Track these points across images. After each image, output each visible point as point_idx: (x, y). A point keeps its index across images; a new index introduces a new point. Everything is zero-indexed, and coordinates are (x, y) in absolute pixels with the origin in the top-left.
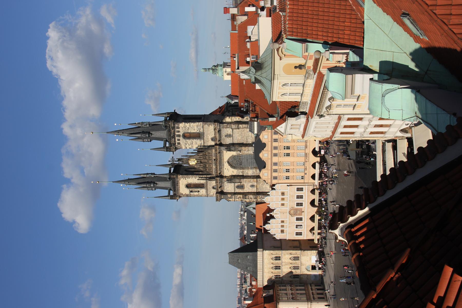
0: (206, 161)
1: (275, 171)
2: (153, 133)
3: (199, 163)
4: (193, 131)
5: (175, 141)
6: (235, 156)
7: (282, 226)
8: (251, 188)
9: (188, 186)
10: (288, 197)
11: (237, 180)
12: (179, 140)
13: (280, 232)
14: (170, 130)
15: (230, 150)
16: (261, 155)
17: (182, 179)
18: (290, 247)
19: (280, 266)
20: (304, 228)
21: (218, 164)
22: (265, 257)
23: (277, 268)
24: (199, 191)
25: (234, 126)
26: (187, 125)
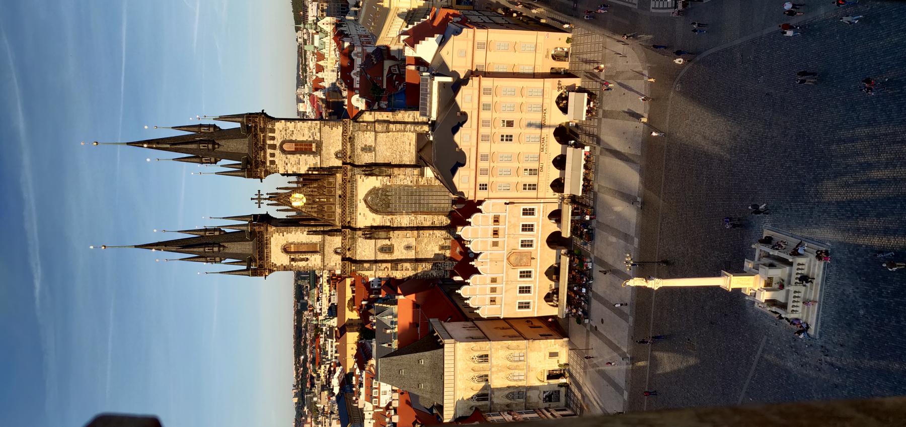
1: (485, 172)
2: (222, 142)
4: (300, 138)
5: (265, 157)
6: (379, 189)
7: (493, 290)
8: (405, 252)
11: (383, 234)
12: (273, 155)
13: (488, 301)
14: (256, 135)
15: (371, 175)
16: (457, 138)
17: (276, 235)
20: (535, 292)
22: (458, 357)
24: (307, 259)
25: (379, 127)
26: (291, 125)
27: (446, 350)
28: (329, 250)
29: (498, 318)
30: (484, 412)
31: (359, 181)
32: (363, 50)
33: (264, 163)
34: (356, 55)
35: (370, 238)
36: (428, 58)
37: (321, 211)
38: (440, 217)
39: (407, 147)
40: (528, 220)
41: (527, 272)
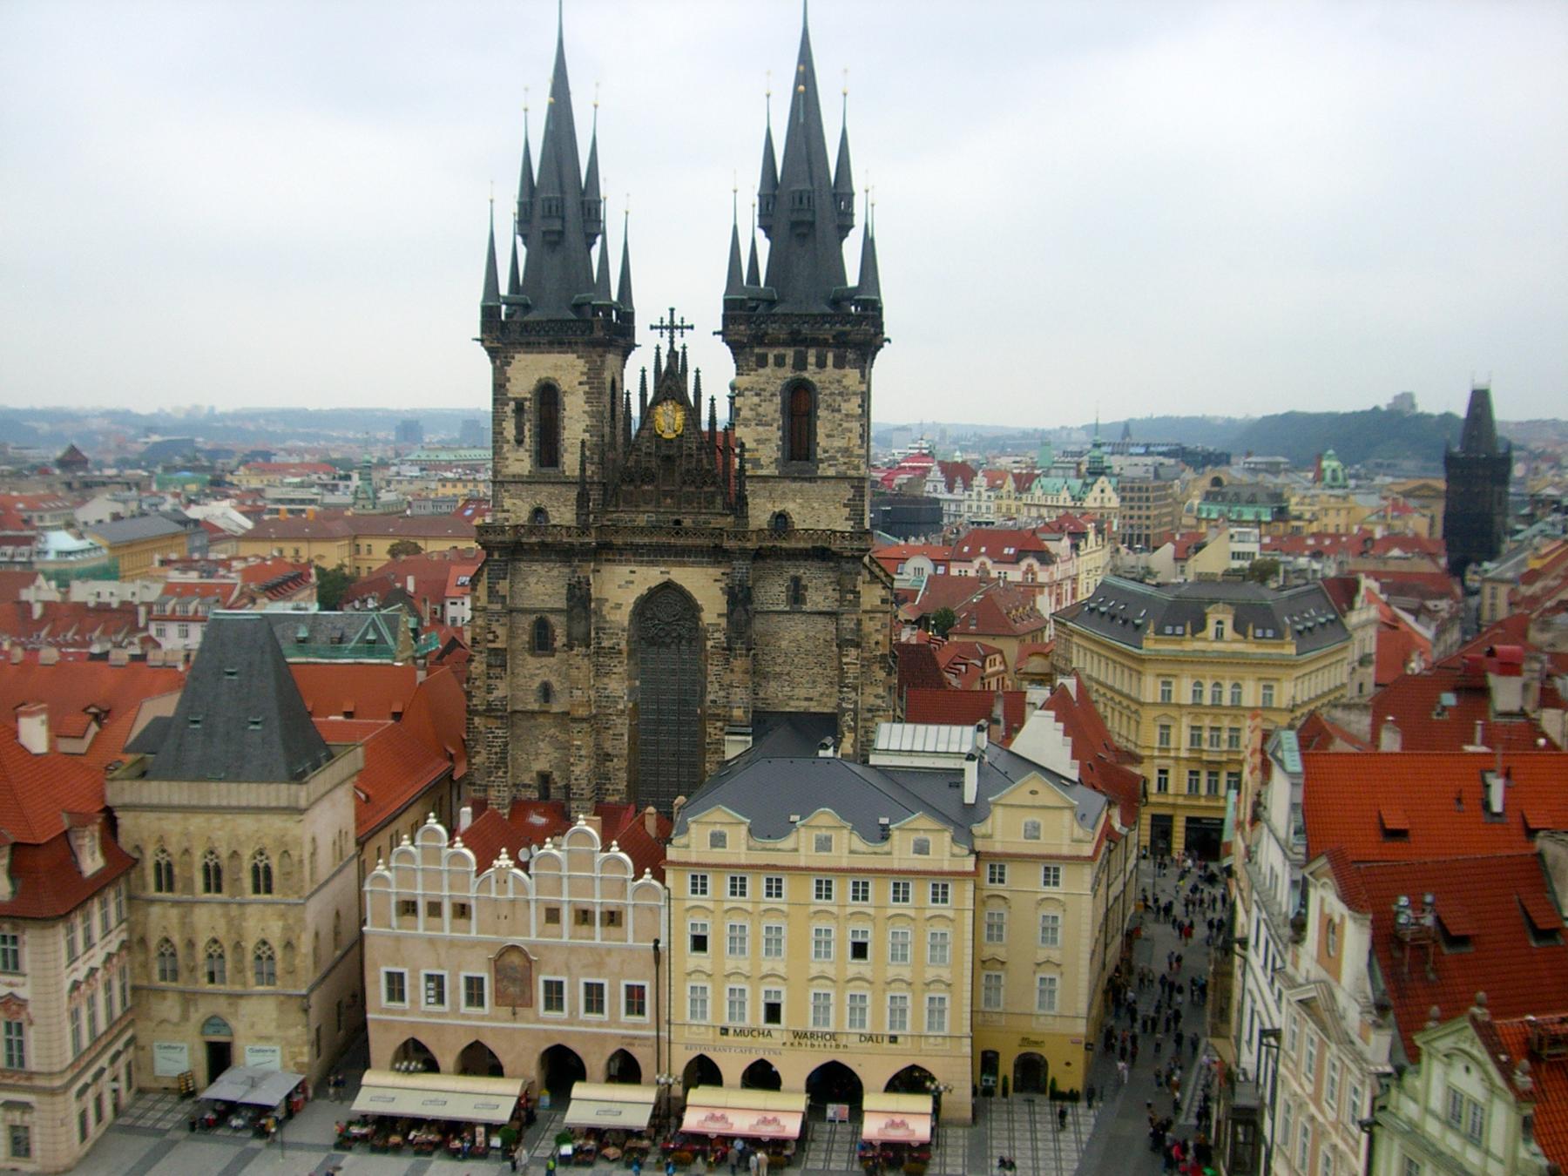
1: (738, 887)
3: (664, 451)
4: (821, 431)
5: (774, 343)
6: (699, 619)
7: (435, 909)
8: (536, 684)
9: (548, 395)
10: (598, 941)
12: (780, 361)
13: (407, 893)
16: (825, 817)
18: (317, 935)
19: (219, 889)
23: (214, 878)
24: (520, 442)
26: (853, 406)
27: (284, 786)
28: (542, 496)
29: (363, 922)
30: (128, 881)
31: (716, 572)
32: (1042, 586)
33: (761, 344)
34: (1030, 569)
35: (571, 596)
36: (1022, 744)
38: (623, 775)
39: (801, 692)
40: (616, 999)
41: (481, 997)
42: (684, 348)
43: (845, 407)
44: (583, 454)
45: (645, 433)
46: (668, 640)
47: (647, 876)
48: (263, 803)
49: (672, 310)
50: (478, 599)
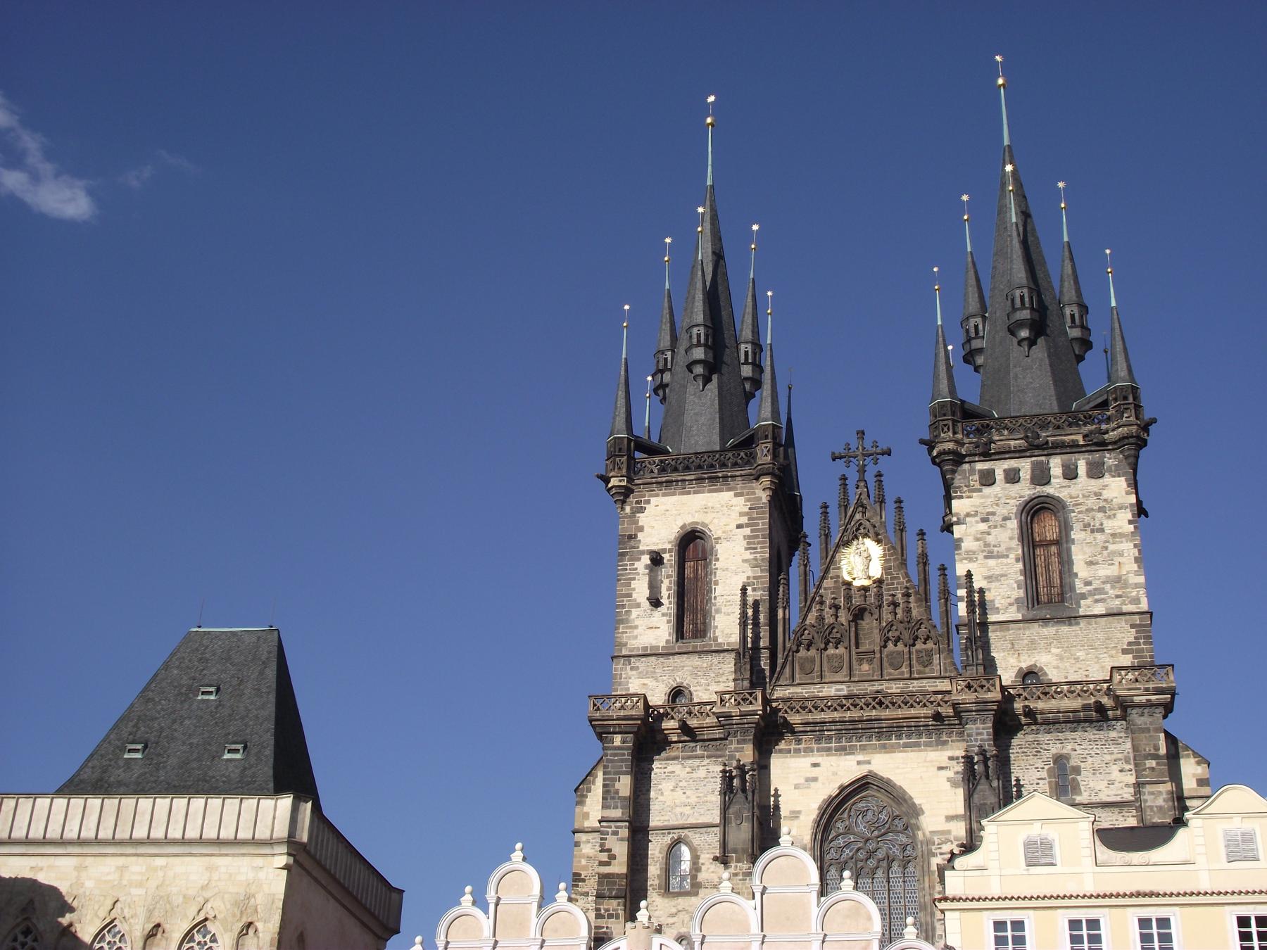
0: (872, 640)
3: (857, 601)
4: (1079, 556)
12: (1012, 477)
15: (970, 777)
21: (855, 714)
24: (655, 602)
26: (1123, 521)
27: (267, 803)
31: (940, 756)
33: (987, 456)
37: (829, 637)
42: (879, 475)
43: (1109, 525)
44: (744, 604)
45: (828, 583)
46: (872, 863)
47: (910, 932)
48: (227, 834)
49: (861, 434)
50: (586, 816)
